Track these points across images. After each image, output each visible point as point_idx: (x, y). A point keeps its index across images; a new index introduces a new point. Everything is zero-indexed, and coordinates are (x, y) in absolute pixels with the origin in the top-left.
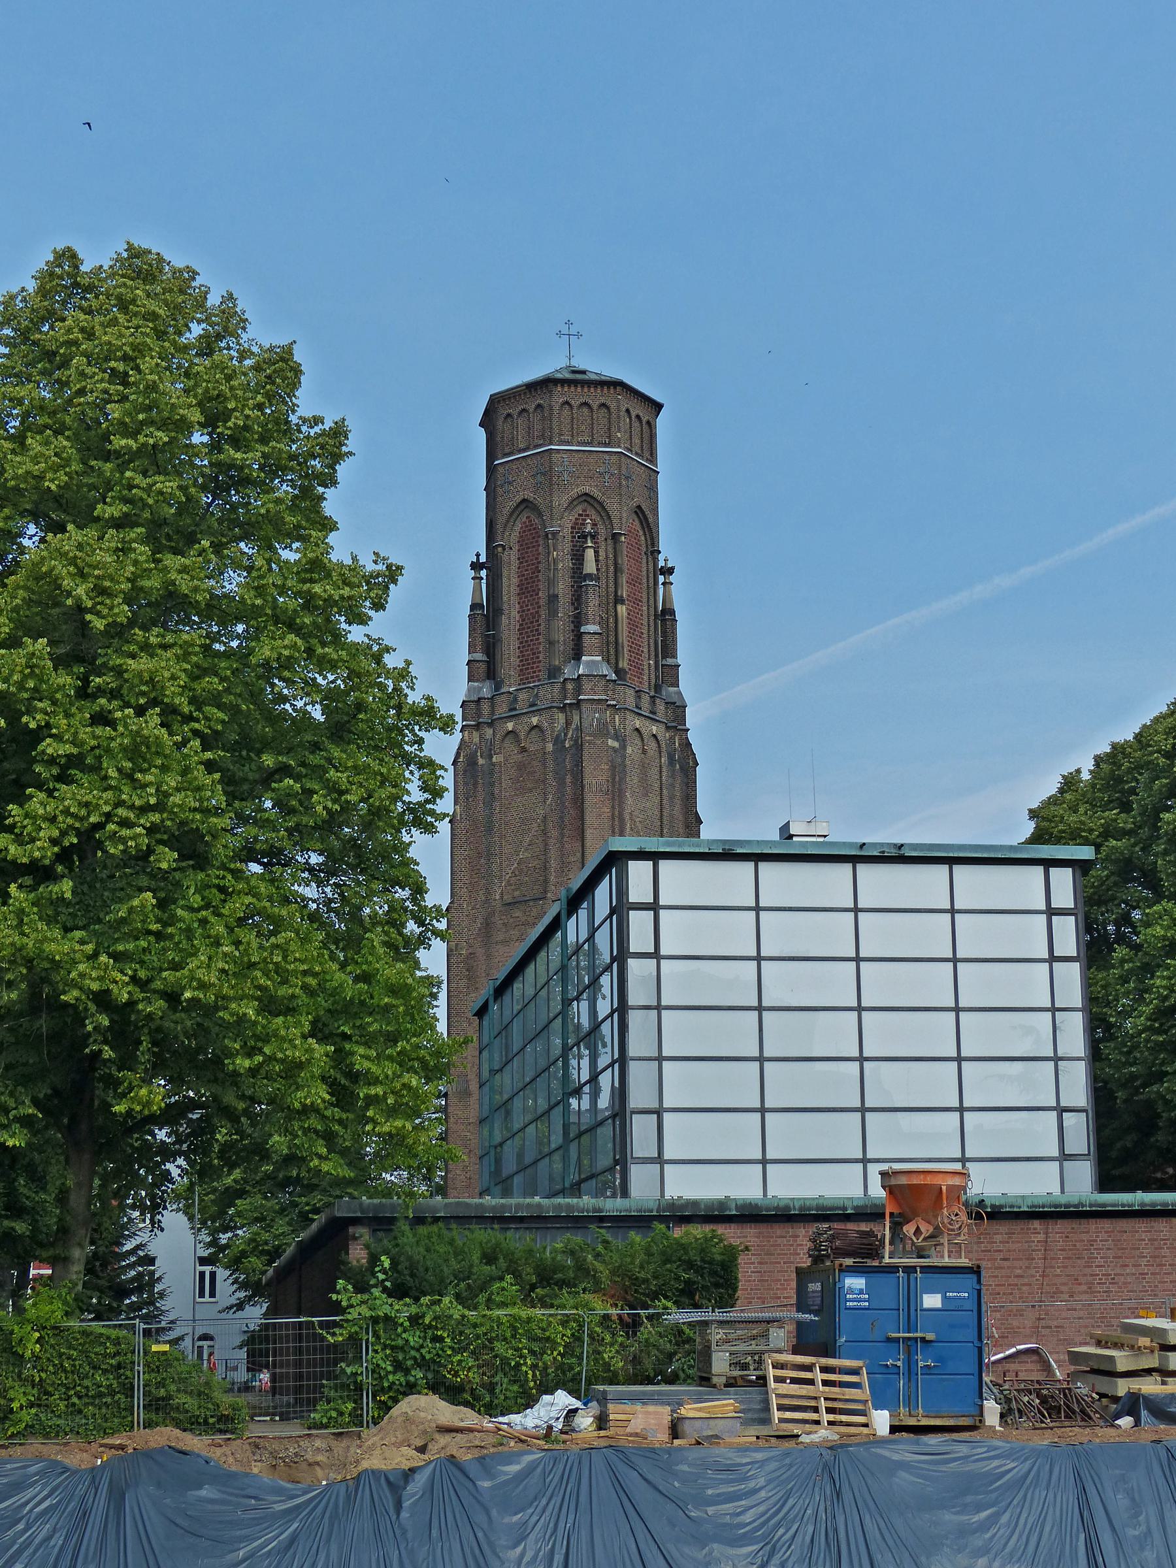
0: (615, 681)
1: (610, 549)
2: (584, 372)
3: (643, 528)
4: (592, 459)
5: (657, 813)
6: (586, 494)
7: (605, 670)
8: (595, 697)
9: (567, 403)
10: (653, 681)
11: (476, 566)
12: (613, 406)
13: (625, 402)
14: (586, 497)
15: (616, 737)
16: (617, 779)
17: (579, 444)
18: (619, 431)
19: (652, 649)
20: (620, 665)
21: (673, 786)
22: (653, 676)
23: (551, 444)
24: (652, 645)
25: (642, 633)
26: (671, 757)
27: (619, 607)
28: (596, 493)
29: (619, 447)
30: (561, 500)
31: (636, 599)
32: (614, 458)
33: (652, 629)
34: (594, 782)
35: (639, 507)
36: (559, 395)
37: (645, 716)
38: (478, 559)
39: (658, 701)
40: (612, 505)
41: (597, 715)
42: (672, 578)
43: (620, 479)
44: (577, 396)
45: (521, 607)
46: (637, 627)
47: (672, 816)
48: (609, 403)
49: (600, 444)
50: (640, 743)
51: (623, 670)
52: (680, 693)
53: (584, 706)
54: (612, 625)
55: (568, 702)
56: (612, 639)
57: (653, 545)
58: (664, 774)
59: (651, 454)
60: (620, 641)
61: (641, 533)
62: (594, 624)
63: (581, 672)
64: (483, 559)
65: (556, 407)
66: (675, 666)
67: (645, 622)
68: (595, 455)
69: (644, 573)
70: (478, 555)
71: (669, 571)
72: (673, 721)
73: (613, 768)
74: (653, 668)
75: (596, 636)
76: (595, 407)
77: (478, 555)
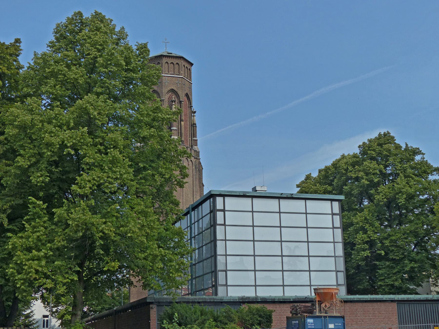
1: (179, 105)
2: (171, 54)
4: (174, 79)
6: (172, 89)
9: (167, 62)
12: (180, 63)
13: (184, 63)
14: (173, 91)
17: (170, 74)
18: (182, 71)
19: (190, 135)
22: (190, 143)
27: (182, 122)
28: (175, 89)
29: (182, 76)
30: (165, 90)
32: (180, 79)
33: (190, 129)
35: (187, 93)
36: (164, 60)
40: (180, 93)
42: (195, 115)
44: (170, 60)
47: (196, 184)
48: (179, 63)
49: (176, 75)
57: (191, 104)
59: (190, 78)
60: (182, 132)
61: (187, 101)
62: (175, 127)
65: (164, 64)
68: (175, 78)
69: (188, 113)
71: (195, 112)
76: (175, 64)
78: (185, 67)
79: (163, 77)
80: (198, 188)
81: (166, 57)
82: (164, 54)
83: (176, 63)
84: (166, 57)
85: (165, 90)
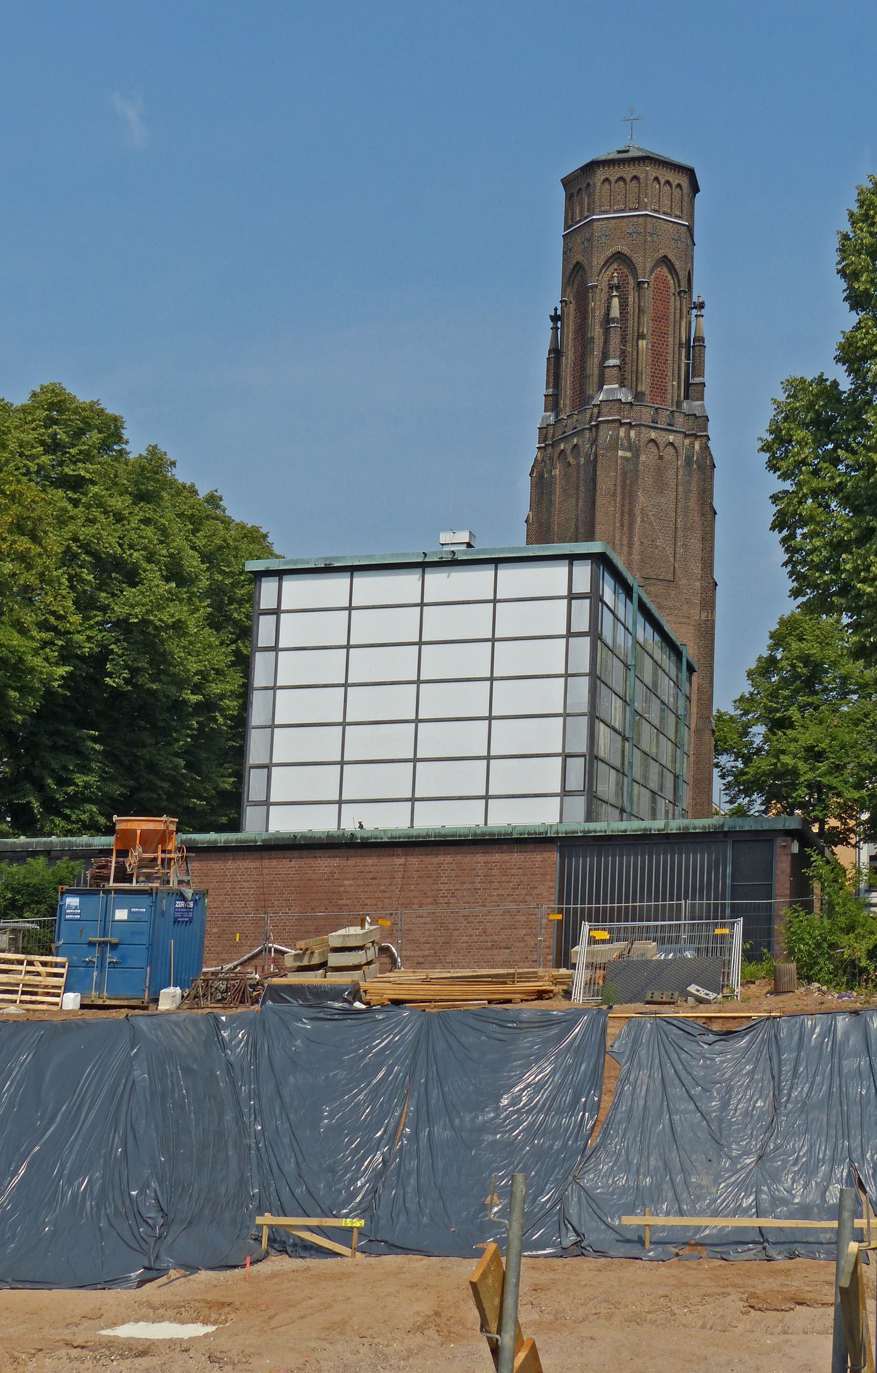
0: (630, 403)
3: (671, 274)
5: (672, 506)
6: (618, 252)
7: (625, 395)
8: (610, 418)
10: (676, 398)
11: (555, 318)
15: (629, 448)
16: (628, 482)
19: (676, 372)
20: (639, 390)
21: (689, 483)
22: (676, 395)
23: (594, 215)
24: (676, 369)
25: (667, 360)
26: (689, 461)
31: (662, 333)
33: (677, 356)
34: (604, 487)
37: (661, 429)
38: (556, 312)
39: (676, 414)
41: (610, 432)
43: (645, 236)
45: (575, 349)
46: (661, 355)
48: (639, 175)
50: (656, 451)
51: (643, 394)
52: (703, 406)
53: (601, 427)
54: (635, 357)
55: (593, 423)
56: (634, 368)
58: (681, 472)
60: (640, 369)
62: (614, 358)
63: (600, 398)
64: (559, 312)
65: (599, 184)
66: (700, 383)
67: (670, 351)
69: (673, 310)
70: (556, 309)
71: (701, 306)
72: (693, 429)
73: (624, 474)
74: (676, 387)
75: (615, 369)
77: (556, 309)
78: (659, 183)
79: (595, 223)
80: (696, 519)
81: (604, 166)
82: (611, 157)
83: (630, 176)
84: (604, 166)
85: (598, 260)
